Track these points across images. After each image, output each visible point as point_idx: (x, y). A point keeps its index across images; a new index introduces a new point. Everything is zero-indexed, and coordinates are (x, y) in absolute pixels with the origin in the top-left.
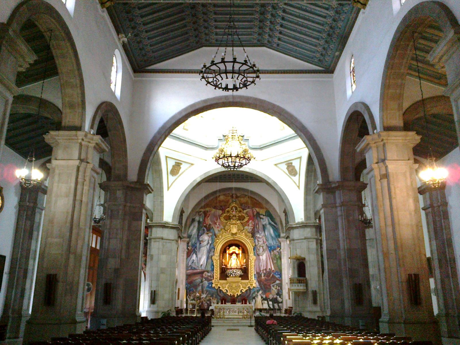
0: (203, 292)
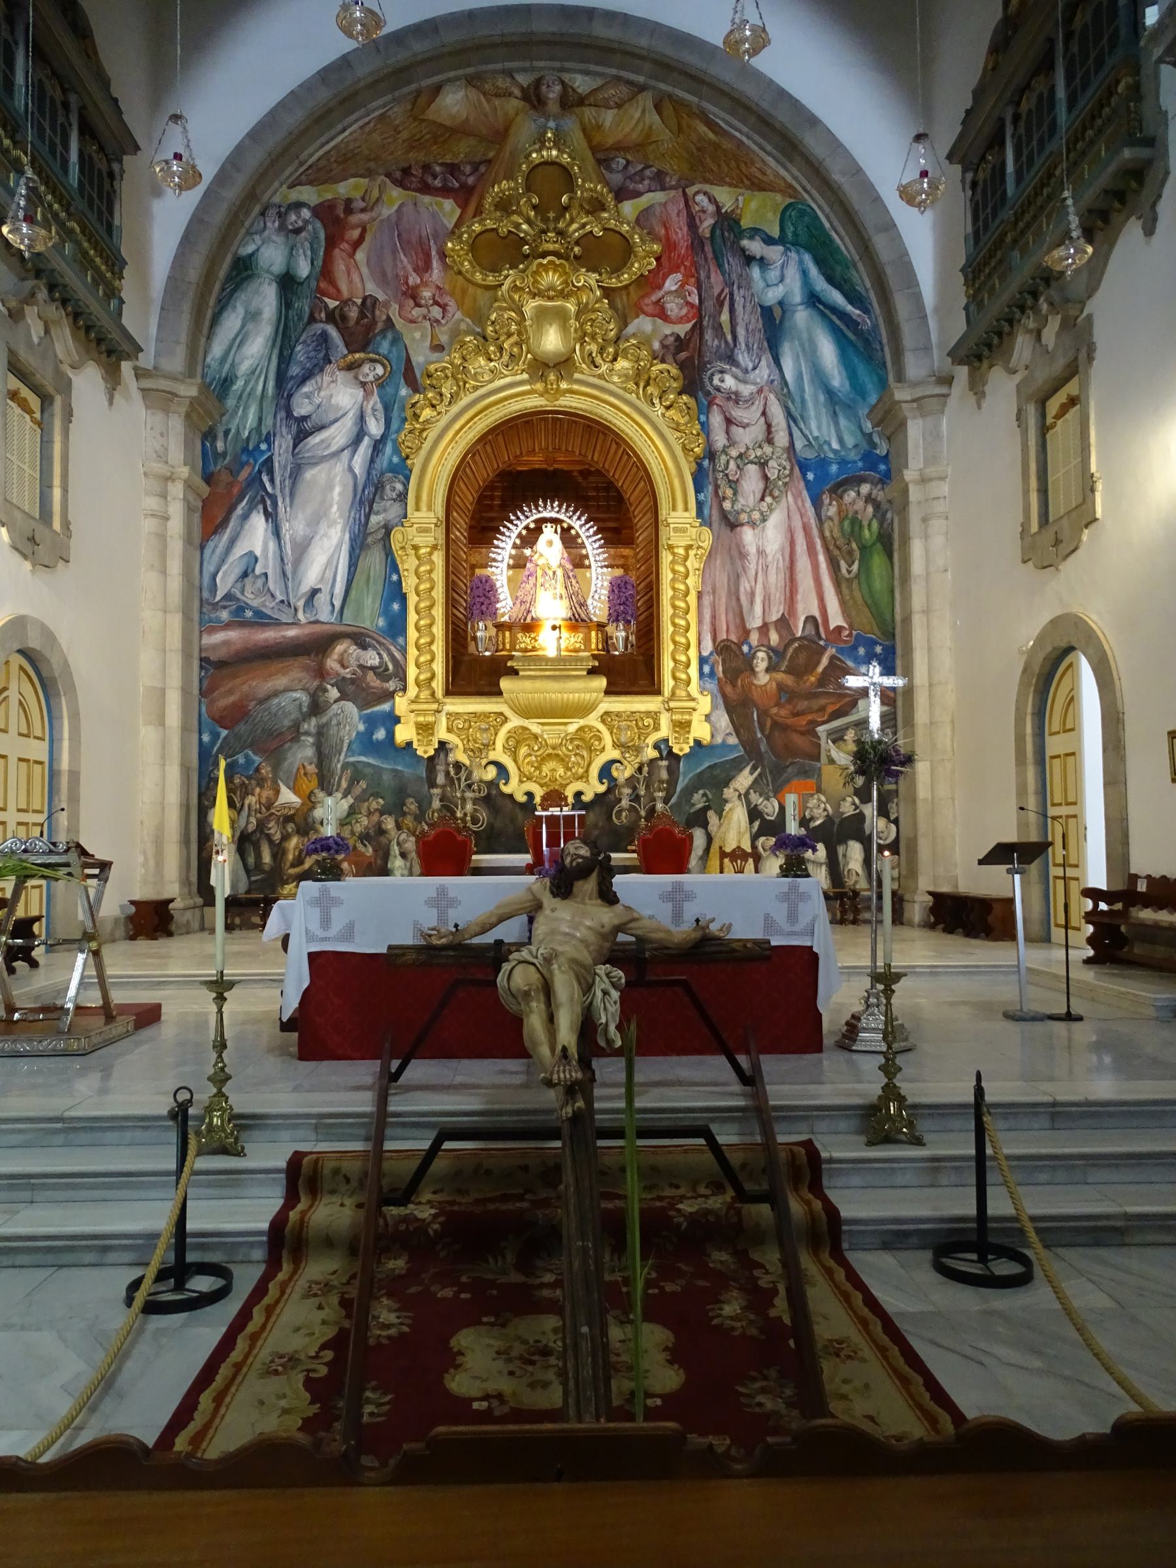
0: (325, 783)
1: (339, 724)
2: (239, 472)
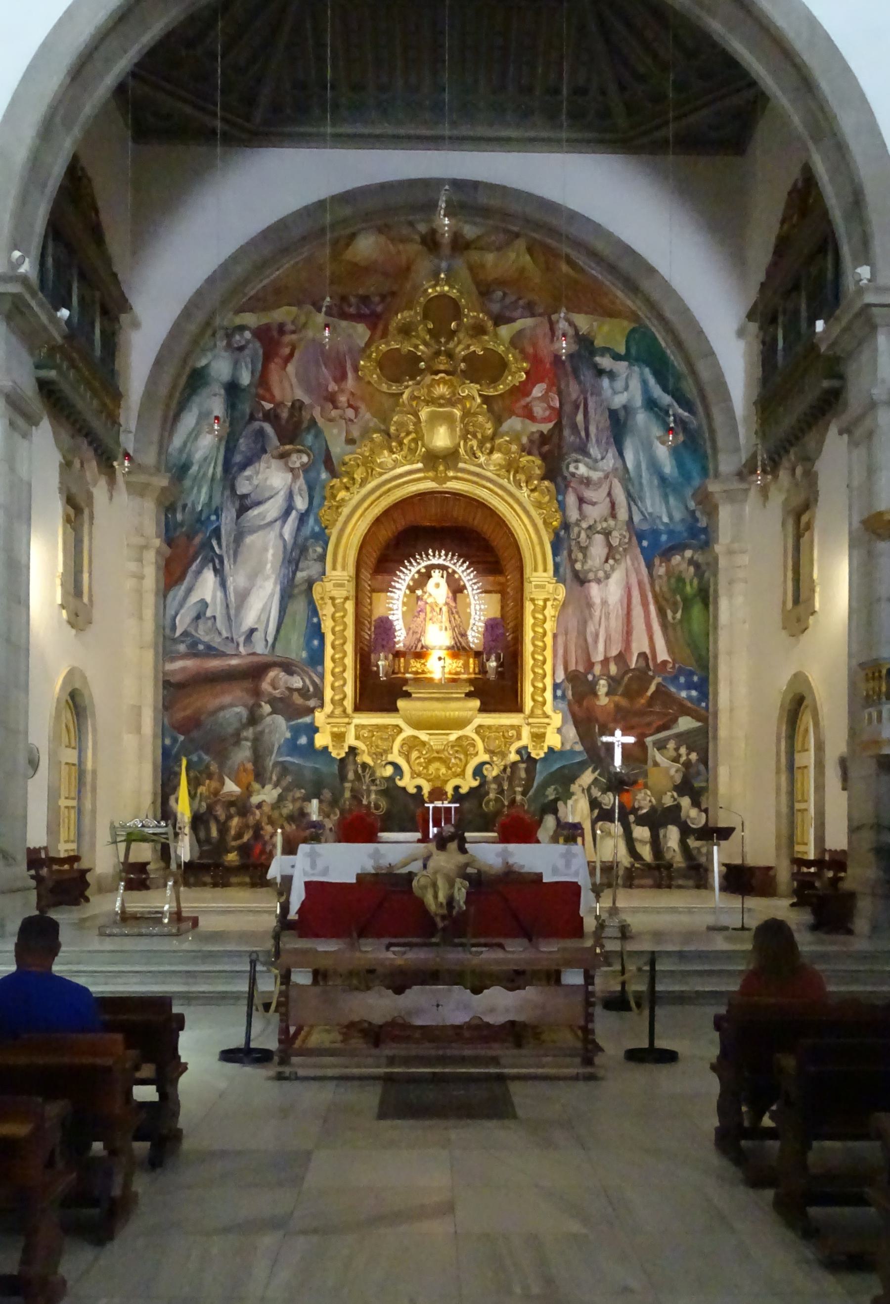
0: (260, 776)
1: (270, 732)
2: (193, 538)
